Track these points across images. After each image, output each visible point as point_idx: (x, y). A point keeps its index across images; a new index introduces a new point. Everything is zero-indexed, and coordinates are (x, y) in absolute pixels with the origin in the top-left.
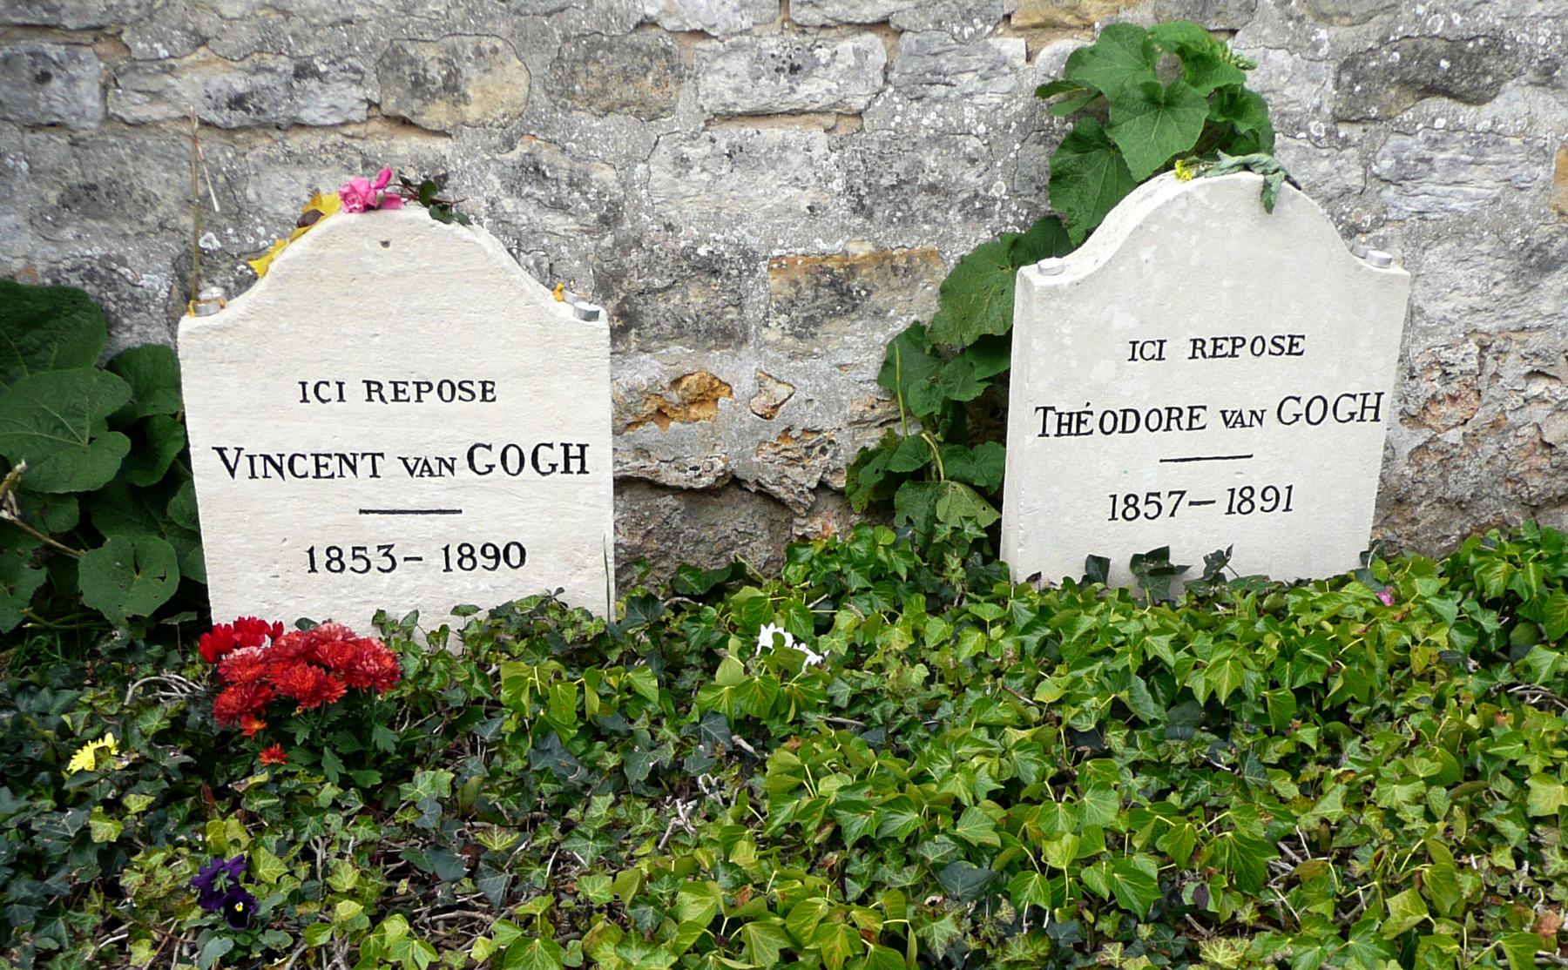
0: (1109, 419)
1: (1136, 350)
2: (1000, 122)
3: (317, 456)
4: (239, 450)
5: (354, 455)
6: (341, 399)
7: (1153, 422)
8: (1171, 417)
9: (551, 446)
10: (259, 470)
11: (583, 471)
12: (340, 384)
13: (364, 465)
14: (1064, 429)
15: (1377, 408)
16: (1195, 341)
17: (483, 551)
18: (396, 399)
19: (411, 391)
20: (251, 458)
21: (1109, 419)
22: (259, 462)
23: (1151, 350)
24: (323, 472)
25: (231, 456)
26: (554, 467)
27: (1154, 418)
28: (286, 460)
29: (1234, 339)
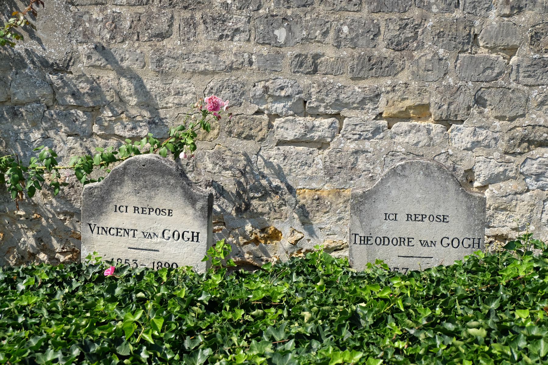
0: (378, 240)
2: (378, 148)
3: (117, 229)
4: (95, 225)
6: (126, 211)
8: (401, 241)
9: (188, 232)
10: (100, 232)
11: (197, 241)
12: (127, 207)
13: (131, 233)
14: (362, 242)
15: (479, 244)
16: (408, 215)
17: (165, 265)
18: (143, 213)
19: (147, 211)
20: (98, 228)
21: (378, 240)
22: (100, 229)
23: (392, 217)
24: (119, 234)
25: (92, 227)
26: (189, 239)
28: (108, 229)
29: (422, 215)
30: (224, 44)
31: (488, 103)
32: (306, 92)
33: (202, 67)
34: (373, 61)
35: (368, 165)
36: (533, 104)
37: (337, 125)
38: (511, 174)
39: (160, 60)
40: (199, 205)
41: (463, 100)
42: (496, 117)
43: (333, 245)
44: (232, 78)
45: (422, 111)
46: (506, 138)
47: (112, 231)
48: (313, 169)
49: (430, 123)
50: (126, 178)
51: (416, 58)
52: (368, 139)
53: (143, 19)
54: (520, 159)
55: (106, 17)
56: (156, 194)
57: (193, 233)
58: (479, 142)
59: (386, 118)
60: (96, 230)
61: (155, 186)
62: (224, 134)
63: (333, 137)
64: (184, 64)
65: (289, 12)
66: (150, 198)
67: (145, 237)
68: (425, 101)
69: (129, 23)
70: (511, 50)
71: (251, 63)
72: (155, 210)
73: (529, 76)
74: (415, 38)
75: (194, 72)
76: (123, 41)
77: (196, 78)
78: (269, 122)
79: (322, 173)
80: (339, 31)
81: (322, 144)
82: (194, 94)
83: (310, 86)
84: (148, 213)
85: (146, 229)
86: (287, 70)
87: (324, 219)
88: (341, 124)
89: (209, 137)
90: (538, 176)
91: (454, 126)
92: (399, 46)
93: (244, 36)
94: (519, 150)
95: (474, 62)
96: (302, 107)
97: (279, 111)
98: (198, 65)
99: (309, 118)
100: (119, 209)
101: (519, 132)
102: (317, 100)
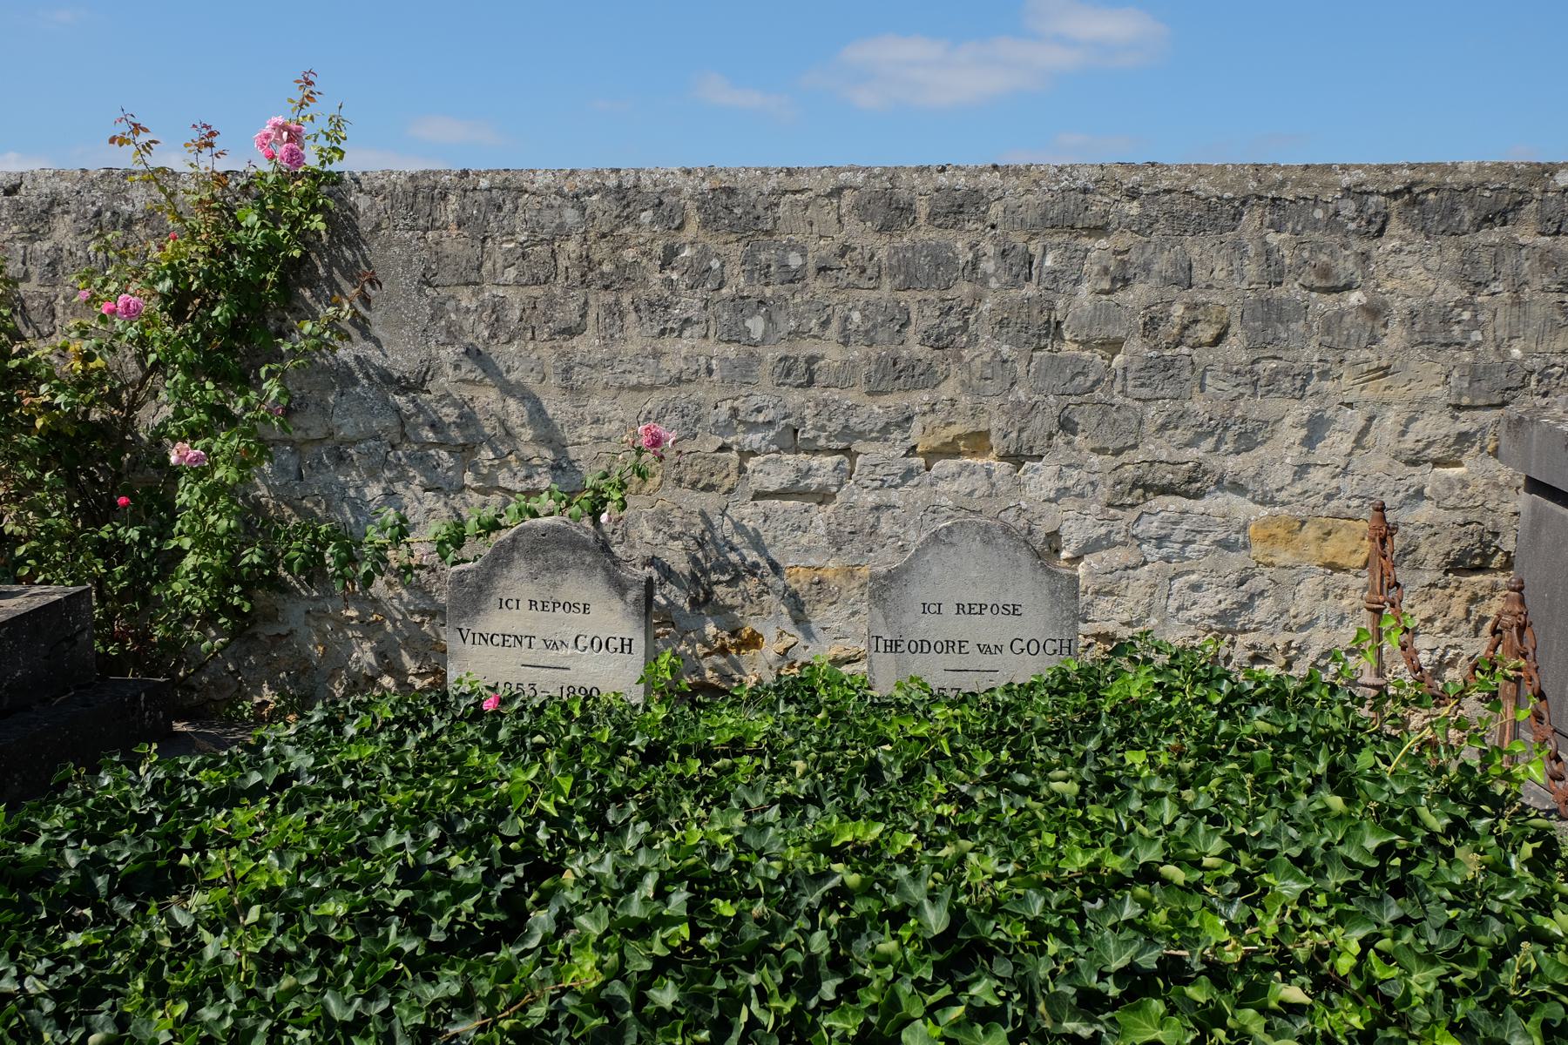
1: (926, 608)
7: (939, 647)
8: (948, 646)
13: (526, 642)
23: (934, 608)
27: (939, 647)
30: (667, 342)
31: (1080, 427)
32: (797, 415)
33: (633, 379)
34: (900, 366)
35: (896, 528)
36: (1150, 428)
37: (847, 466)
38: (1119, 538)
39: (568, 370)
40: (631, 595)
41: (1042, 423)
42: (1093, 450)
43: (844, 654)
44: (681, 395)
45: (978, 441)
46: (1110, 482)
48: (811, 535)
49: (991, 460)
50: (516, 555)
51: (967, 359)
52: (896, 487)
53: (541, 307)
54: (1132, 514)
55: (482, 304)
58: (1066, 489)
59: (922, 454)
61: (561, 567)
62: (670, 484)
63: (841, 485)
64: (606, 376)
65: (768, 292)
66: (555, 586)
68: (983, 427)
69: (518, 313)
70: (1114, 346)
71: (710, 372)
73: (1143, 385)
74: (964, 328)
75: (621, 388)
76: (509, 342)
77: (625, 395)
78: (741, 464)
79: (824, 542)
80: (847, 319)
81: (823, 496)
83: (802, 406)
85: (550, 636)
86: (767, 382)
87: (829, 614)
88: (853, 464)
89: (647, 488)
90: (1161, 541)
91: (1028, 464)
92: (939, 341)
93: (698, 330)
94: (1129, 500)
95: (1057, 364)
96: (791, 439)
97: (755, 446)
98: (628, 376)
99: (802, 456)
101: (1129, 473)
102: (814, 427)
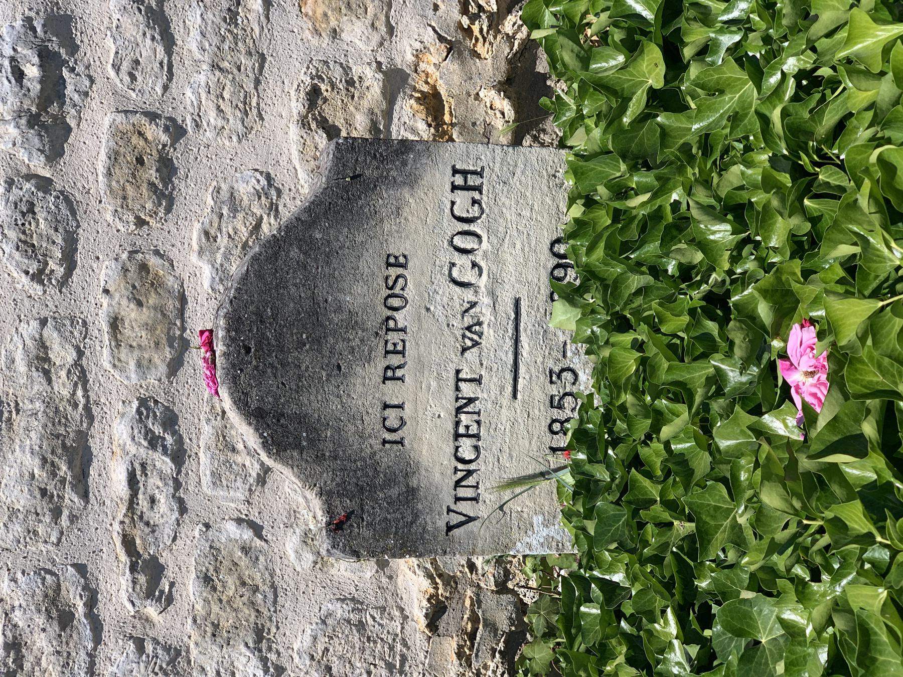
3: (457, 436)
4: (449, 510)
5: (457, 399)
9: (453, 203)
11: (480, 174)
12: (386, 406)
13: (467, 390)
19: (393, 337)
20: (458, 499)
22: (462, 492)
24: (474, 430)
25: (455, 519)
26: (474, 202)
28: (460, 466)
47: (468, 454)
56: (339, 309)
57: (454, 188)
60: (465, 508)
66: (353, 323)
67: (476, 344)
72: (390, 313)
82: (43, 322)
84: (401, 335)
85: (453, 342)
100: (394, 431)
